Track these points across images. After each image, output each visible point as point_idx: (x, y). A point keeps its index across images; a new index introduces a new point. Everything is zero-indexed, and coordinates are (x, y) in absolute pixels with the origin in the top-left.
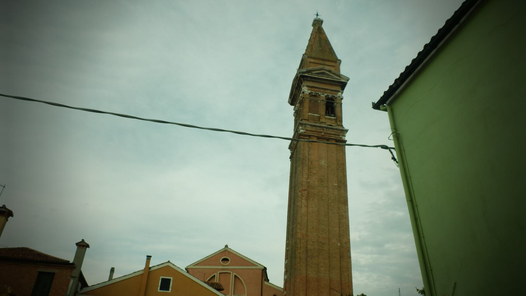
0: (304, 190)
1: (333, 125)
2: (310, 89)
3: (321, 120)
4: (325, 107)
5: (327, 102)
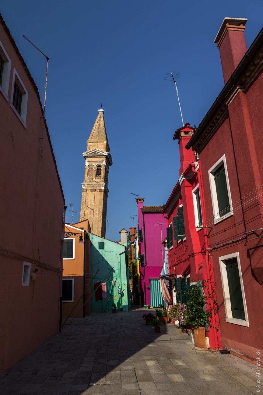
0: (82, 218)
1: (100, 181)
2: (89, 162)
3: (93, 180)
4: (96, 172)
5: (97, 169)
